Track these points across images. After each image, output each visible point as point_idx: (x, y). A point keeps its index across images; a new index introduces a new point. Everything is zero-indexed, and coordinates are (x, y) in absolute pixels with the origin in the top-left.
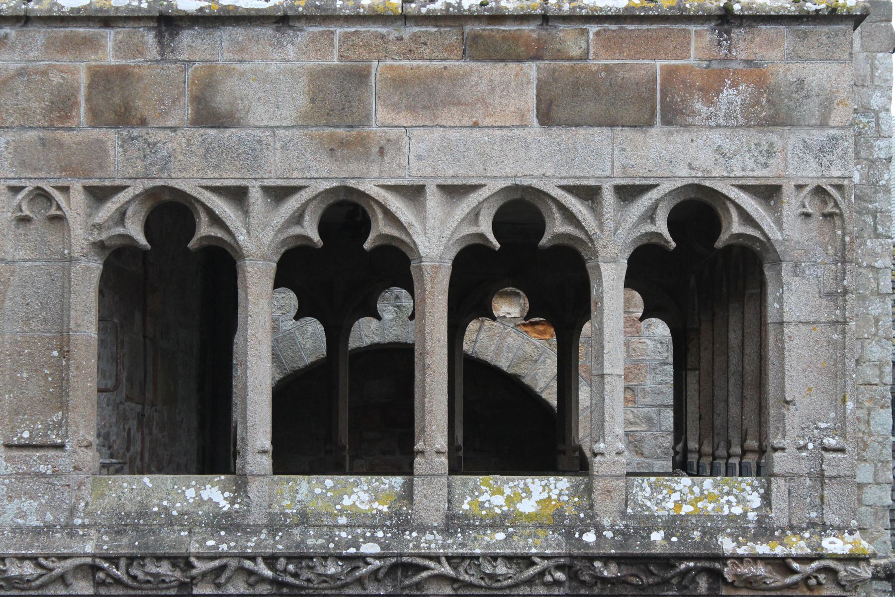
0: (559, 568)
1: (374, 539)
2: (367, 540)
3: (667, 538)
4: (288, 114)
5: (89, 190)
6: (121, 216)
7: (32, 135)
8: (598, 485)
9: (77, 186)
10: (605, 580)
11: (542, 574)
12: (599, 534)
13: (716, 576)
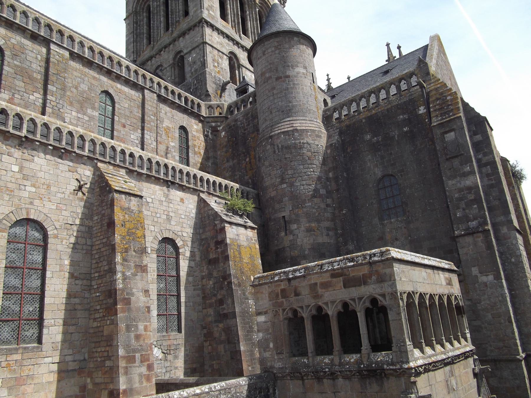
0: (358, 372)
1: (328, 368)
2: (327, 368)
3: (375, 366)
4: (307, 293)
5: (282, 309)
6: (287, 313)
7: (274, 301)
8: (363, 356)
9: (281, 309)
10: (366, 375)
11: (354, 374)
12: (364, 366)
13: (384, 373)
